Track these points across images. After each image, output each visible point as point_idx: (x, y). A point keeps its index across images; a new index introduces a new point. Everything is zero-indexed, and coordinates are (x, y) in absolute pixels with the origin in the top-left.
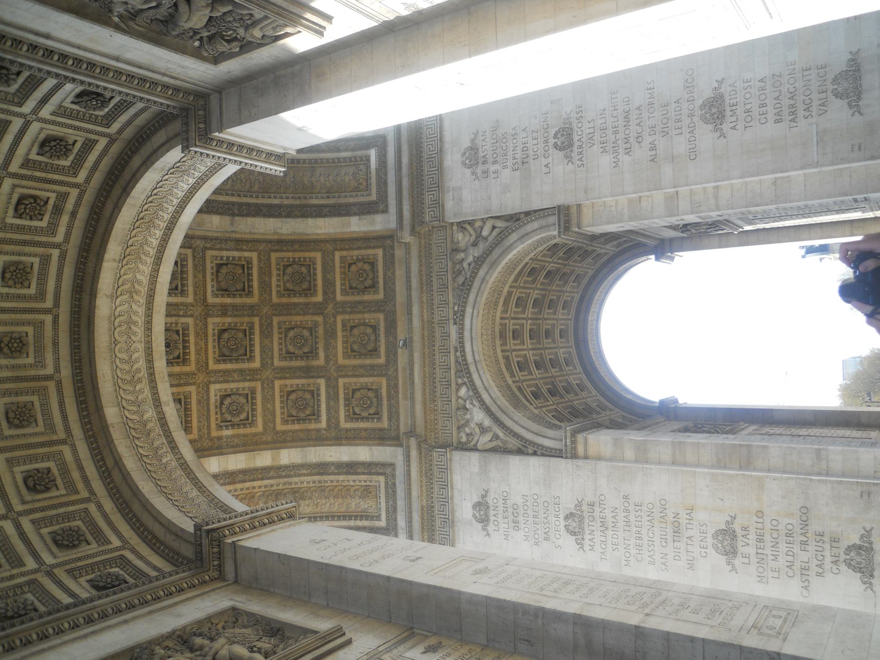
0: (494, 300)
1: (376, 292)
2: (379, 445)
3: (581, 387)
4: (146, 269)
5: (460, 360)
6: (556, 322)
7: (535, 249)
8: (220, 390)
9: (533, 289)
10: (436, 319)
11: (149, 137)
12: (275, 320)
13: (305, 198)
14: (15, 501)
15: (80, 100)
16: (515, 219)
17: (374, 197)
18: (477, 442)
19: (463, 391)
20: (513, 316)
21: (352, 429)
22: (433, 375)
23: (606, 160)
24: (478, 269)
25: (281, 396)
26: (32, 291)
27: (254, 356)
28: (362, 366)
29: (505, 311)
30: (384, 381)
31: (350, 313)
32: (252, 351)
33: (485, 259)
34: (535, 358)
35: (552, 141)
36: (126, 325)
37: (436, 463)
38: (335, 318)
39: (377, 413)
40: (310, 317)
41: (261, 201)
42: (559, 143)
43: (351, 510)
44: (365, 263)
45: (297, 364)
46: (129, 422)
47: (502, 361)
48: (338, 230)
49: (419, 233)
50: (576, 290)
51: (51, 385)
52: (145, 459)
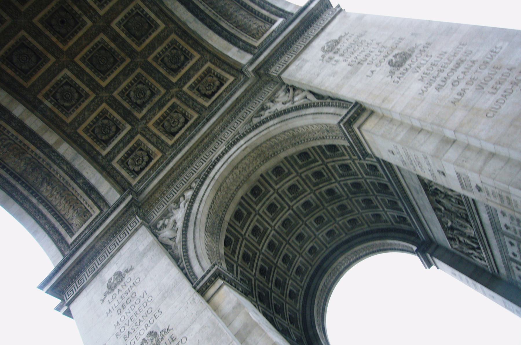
0: (267, 155)
1: (207, 101)
3: (292, 296)
6: (313, 237)
8: (69, 78)
12: (139, 70)
13: (220, 19)
20: (280, 191)
23: (417, 86)
28: (158, 138)
35: (390, 57)
38: (172, 97)
40: (159, 85)
44: (218, 80)
48: (221, 49)
49: (260, 77)
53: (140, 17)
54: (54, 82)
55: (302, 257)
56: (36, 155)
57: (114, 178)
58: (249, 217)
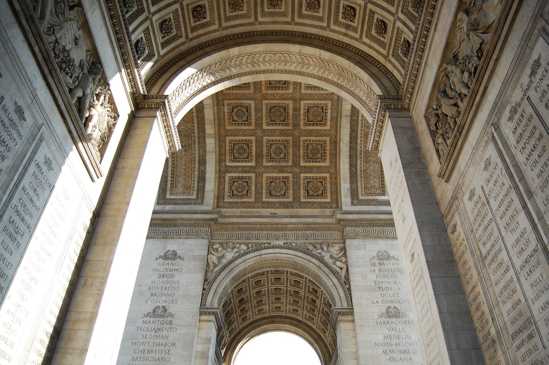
3: (244, 319)
5: (263, 246)
6: (285, 304)
7: (328, 294)
9: (305, 291)
10: (288, 233)
12: (290, 138)
13: (361, 158)
15: (406, 42)
16: (346, 283)
17: (361, 197)
18: (213, 255)
19: (244, 247)
20: (289, 278)
21: (225, 181)
22: (255, 229)
23: (380, 338)
24: (316, 259)
25: (246, 140)
26: (304, 12)
27: (269, 126)
28: (262, 187)
29: (291, 274)
30: (252, 200)
31: (293, 182)
32: (272, 124)
33: (323, 263)
34: (263, 291)
35: (392, 305)
36: (284, 60)
37: (202, 229)
38: (291, 172)
41: (359, 132)
42: (391, 310)
43: (177, 178)
45: (264, 150)
46: (230, 60)
47: (261, 271)
50: (304, 317)
51: (252, 20)
52: (208, 68)
53: (322, 111)
54: (241, 101)
55: (269, 307)
56: (194, 130)
57: (219, 184)
58: (261, 276)
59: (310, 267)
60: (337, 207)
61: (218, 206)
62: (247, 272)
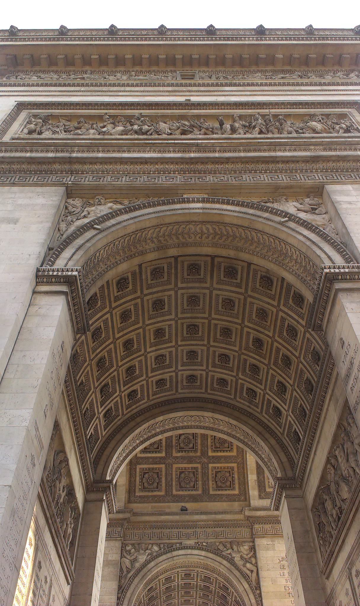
2: (126, 489)
4: (225, 429)
6: (195, 598)
9: (215, 587)
11: (283, 451)
14: (126, 392)
16: (257, 588)
18: (125, 557)
19: (156, 548)
21: (136, 473)
24: (227, 560)
26: (215, 386)
28: (172, 479)
30: (162, 493)
33: (233, 565)
39: (144, 488)
45: (173, 440)
51: (174, 392)
55: (178, 601)
59: (222, 570)
60: (245, 500)
61: (129, 501)
62: (159, 574)
